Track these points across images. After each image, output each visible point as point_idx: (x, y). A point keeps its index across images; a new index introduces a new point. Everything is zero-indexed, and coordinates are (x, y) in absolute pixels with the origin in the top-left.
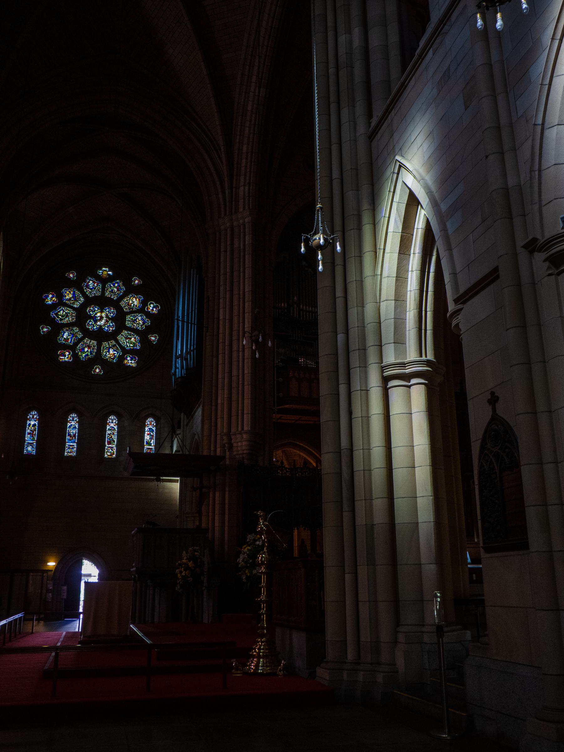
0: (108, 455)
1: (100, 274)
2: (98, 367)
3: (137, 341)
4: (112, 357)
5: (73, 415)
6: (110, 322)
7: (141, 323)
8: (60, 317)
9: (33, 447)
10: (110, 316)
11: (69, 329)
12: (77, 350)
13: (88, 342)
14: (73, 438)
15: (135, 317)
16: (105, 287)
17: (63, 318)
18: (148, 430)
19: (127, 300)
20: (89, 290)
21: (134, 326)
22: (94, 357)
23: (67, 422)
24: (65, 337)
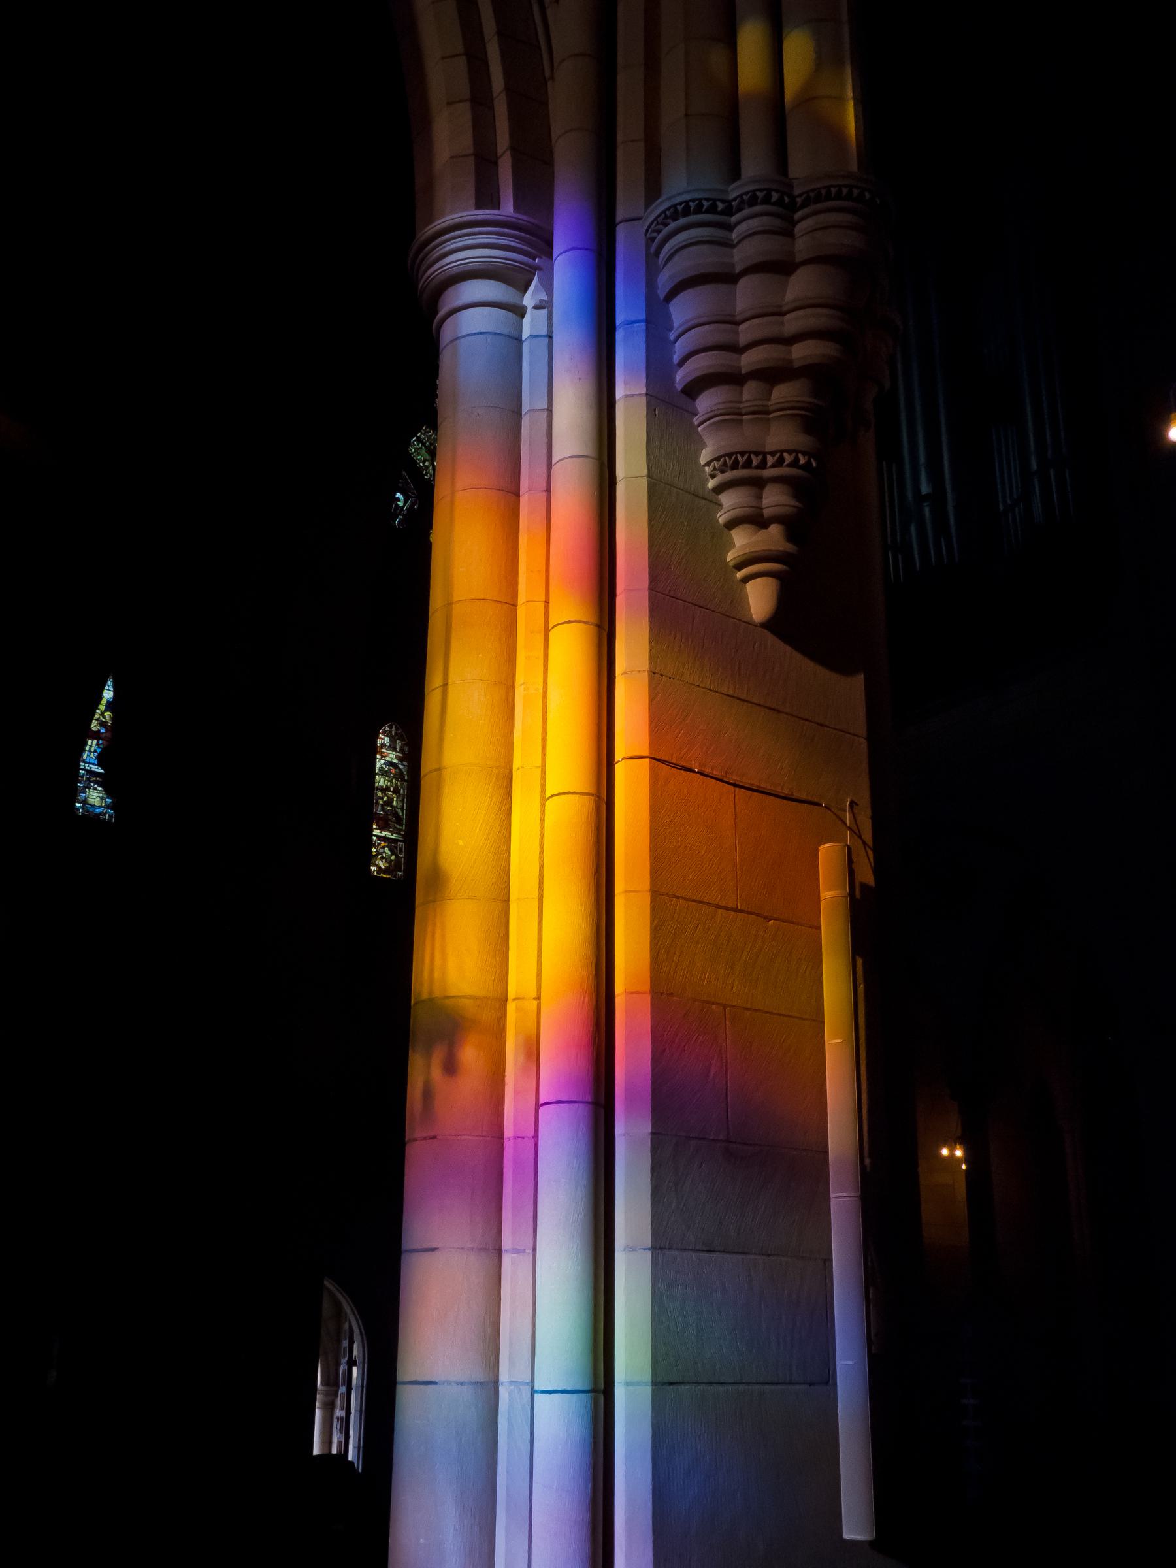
0: (380, 870)
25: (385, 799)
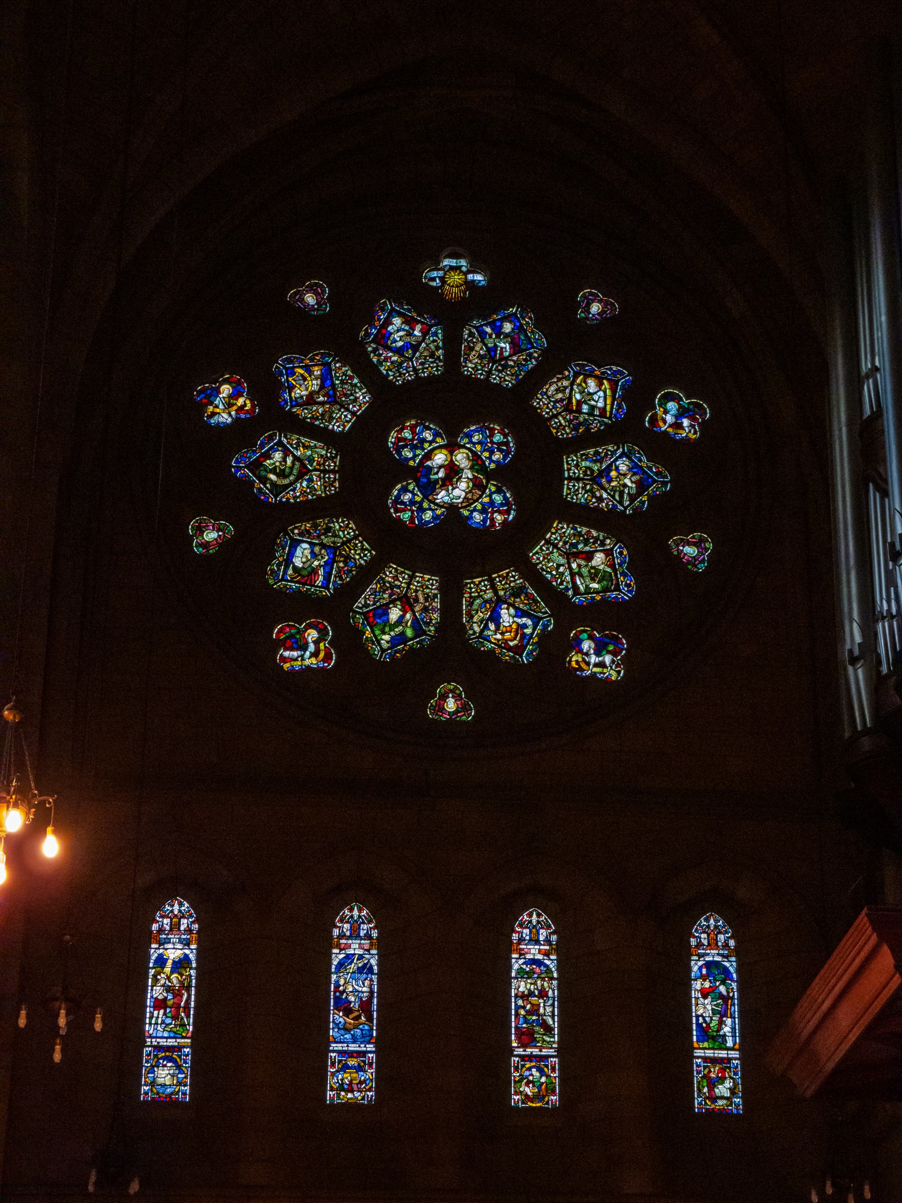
1: (434, 284)
2: (451, 691)
3: (620, 565)
4: (511, 644)
5: (356, 912)
6: (493, 489)
7: (629, 484)
8: (273, 477)
9: (179, 1067)
10: (491, 461)
11: (315, 526)
12: (354, 617)
13: (402, 581)
14: (357, 1018)
15: (601, 461)
16: (460, 339)
17: (286, 482)
18: (704, 971)
19: (558, 390)
20: (390, 354)
21: (600, 499)
22: (431, 643)
23: (328, 943)
24: (299, 564)
25: (528, 1007)
